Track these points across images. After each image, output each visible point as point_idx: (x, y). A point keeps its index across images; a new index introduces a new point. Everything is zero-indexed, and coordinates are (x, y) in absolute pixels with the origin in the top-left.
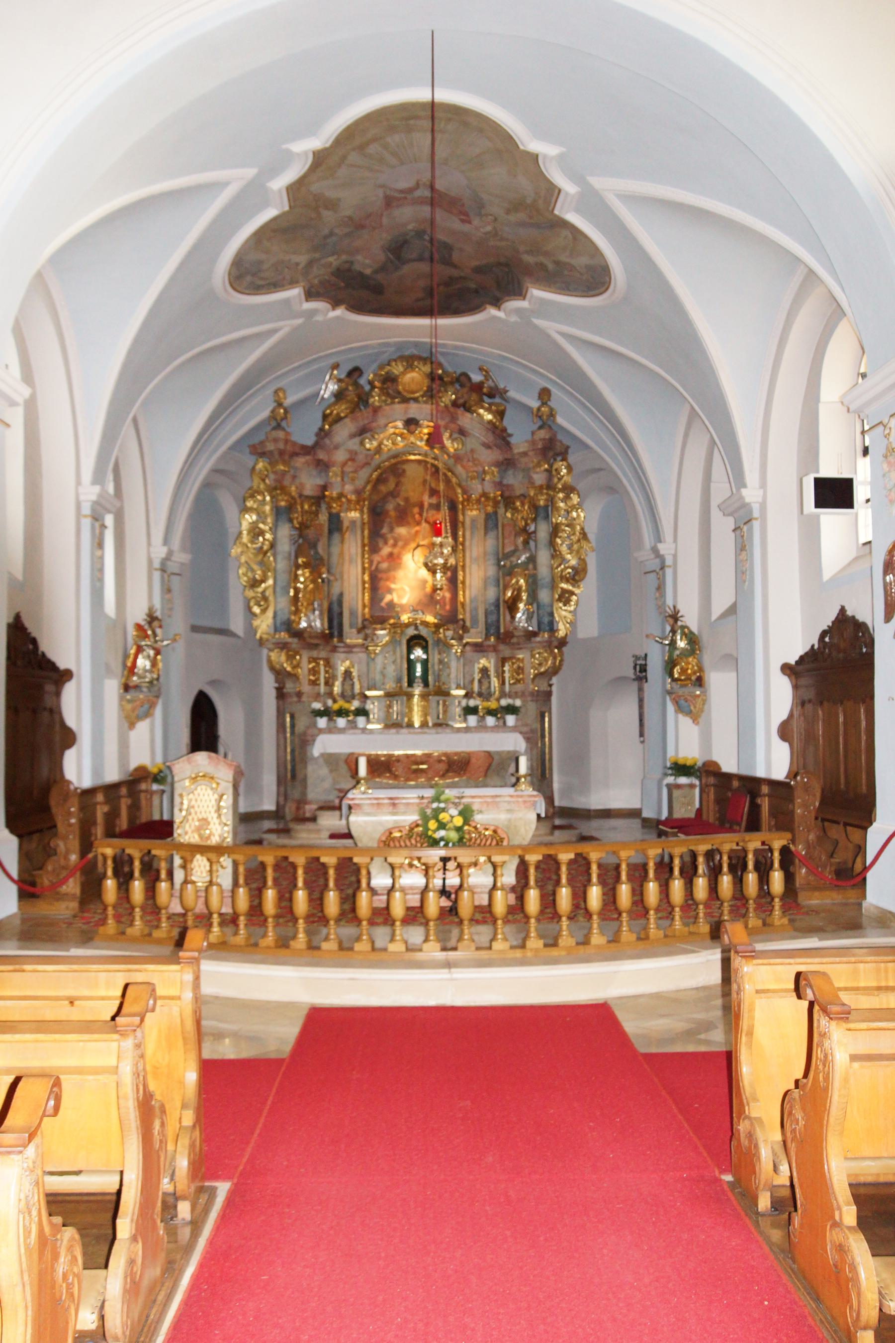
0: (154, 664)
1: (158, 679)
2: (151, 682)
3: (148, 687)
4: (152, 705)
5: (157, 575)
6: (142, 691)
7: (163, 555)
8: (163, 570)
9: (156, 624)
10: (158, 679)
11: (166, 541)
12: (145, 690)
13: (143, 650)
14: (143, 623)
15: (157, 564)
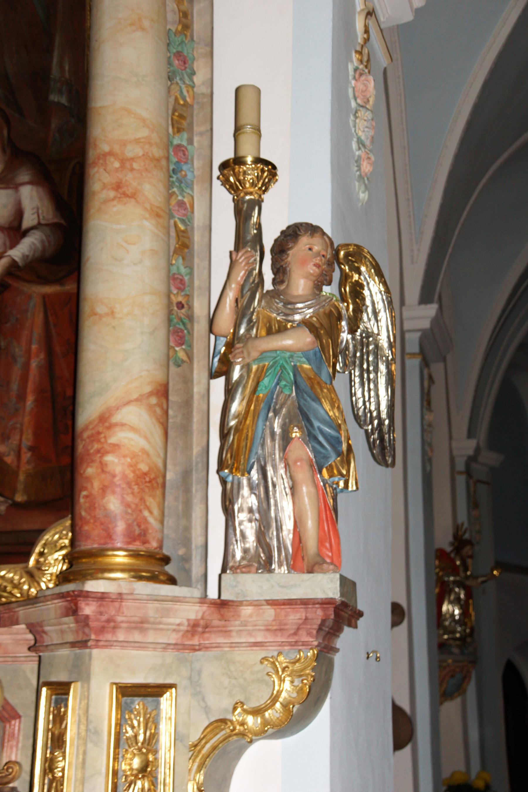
0: (465, 613)
1: (471, 634)
2: (463, 639)
3: (459, 647)
4: (466, 678)
5: (461, 480)
6: (451, 653)
7: (471, 452)
8: (468, 472)
9: (467, 550)
10: (471, 634)
11: (471, 434)
12: (456, 650)
13: (451, 591)
14: (448, 549)
15: (460, 466)
